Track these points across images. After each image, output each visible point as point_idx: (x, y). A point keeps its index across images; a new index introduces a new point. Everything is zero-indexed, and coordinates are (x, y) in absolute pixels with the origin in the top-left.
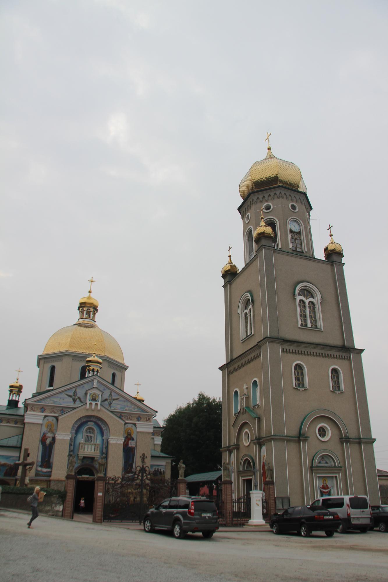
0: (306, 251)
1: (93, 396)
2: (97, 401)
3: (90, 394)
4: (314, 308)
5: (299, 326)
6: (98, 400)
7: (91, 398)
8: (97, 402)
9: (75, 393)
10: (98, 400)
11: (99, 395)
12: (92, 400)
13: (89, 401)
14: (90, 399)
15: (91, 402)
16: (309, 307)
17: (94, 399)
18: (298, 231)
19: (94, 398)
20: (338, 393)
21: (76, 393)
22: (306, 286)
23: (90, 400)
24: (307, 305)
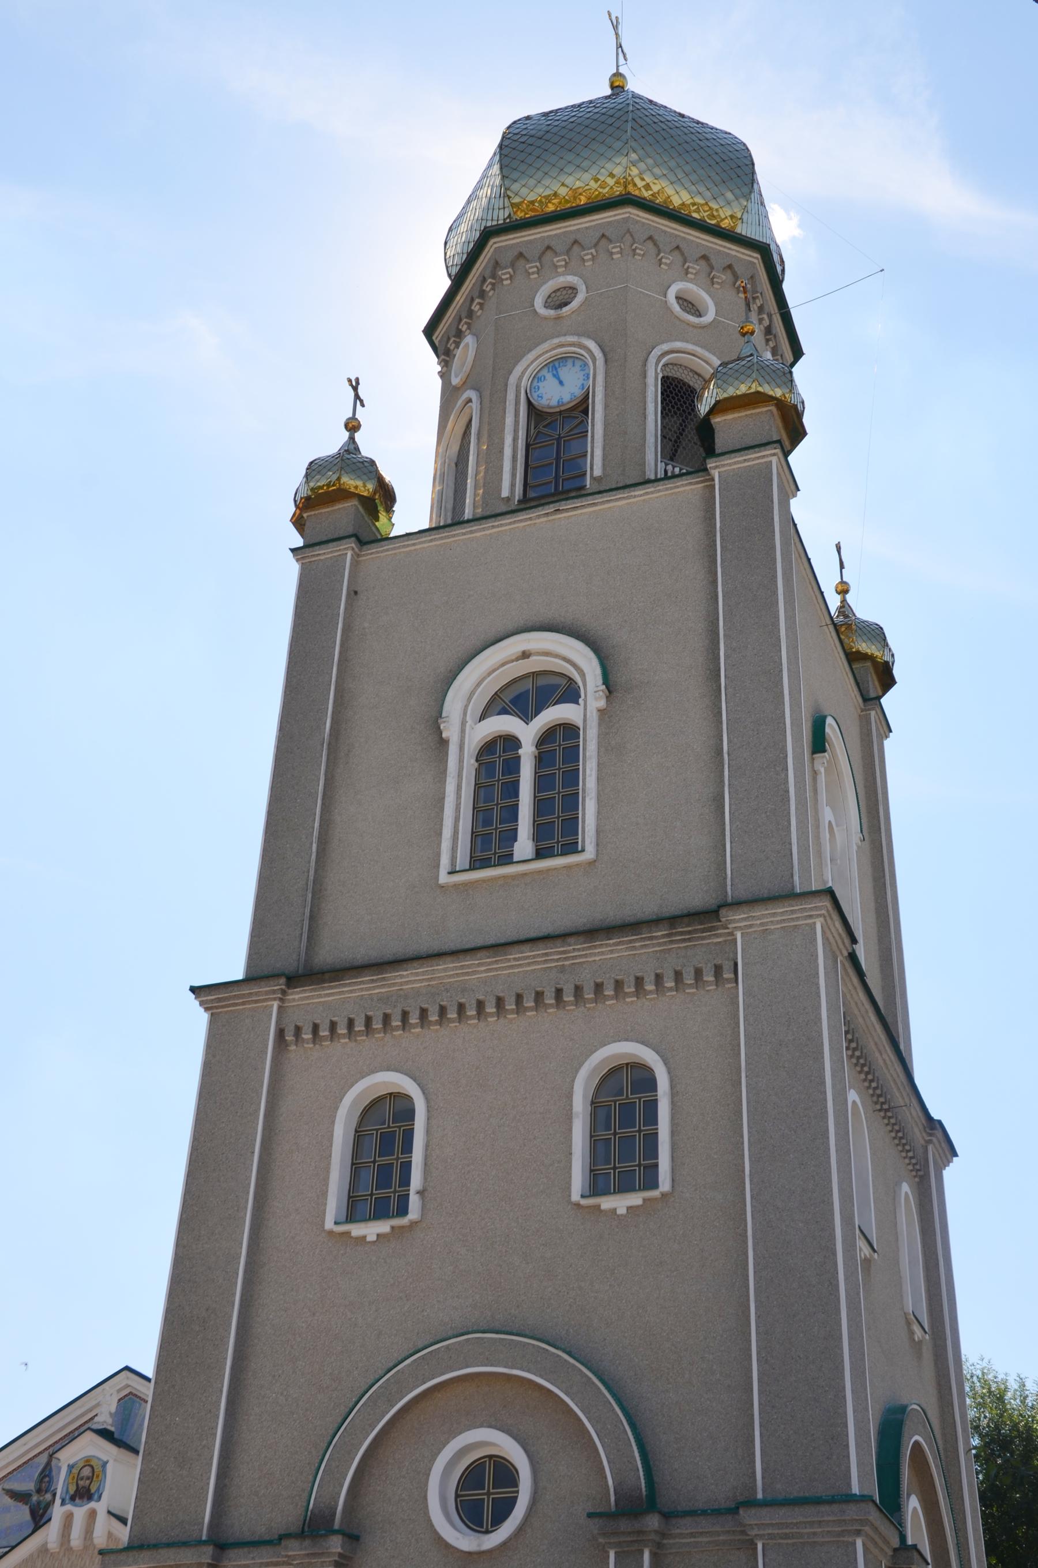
0: (598, 472)
1: (82, 1475)
2: (96, 1497)
3: (71, 1467)
4: (572, 754)
5: (444, 878)
6: (98, 1489)
7: (72, 1491)
8: (93, 1504)
9: (45, 1476)
10: (98, 1489)
11: (105, 1464)
12: (73, 1498)
13: (63, 1503)
14: (67, 1491)
15: (69, 1507)
16: (542, 759)
17: (83, 1487)
18: (579, 393)
19: (81, 1483)
20: (629, 1208)
21: (49, 1475)
22: (525, 655)
23: (68, 1497)
24: (527, 752)
